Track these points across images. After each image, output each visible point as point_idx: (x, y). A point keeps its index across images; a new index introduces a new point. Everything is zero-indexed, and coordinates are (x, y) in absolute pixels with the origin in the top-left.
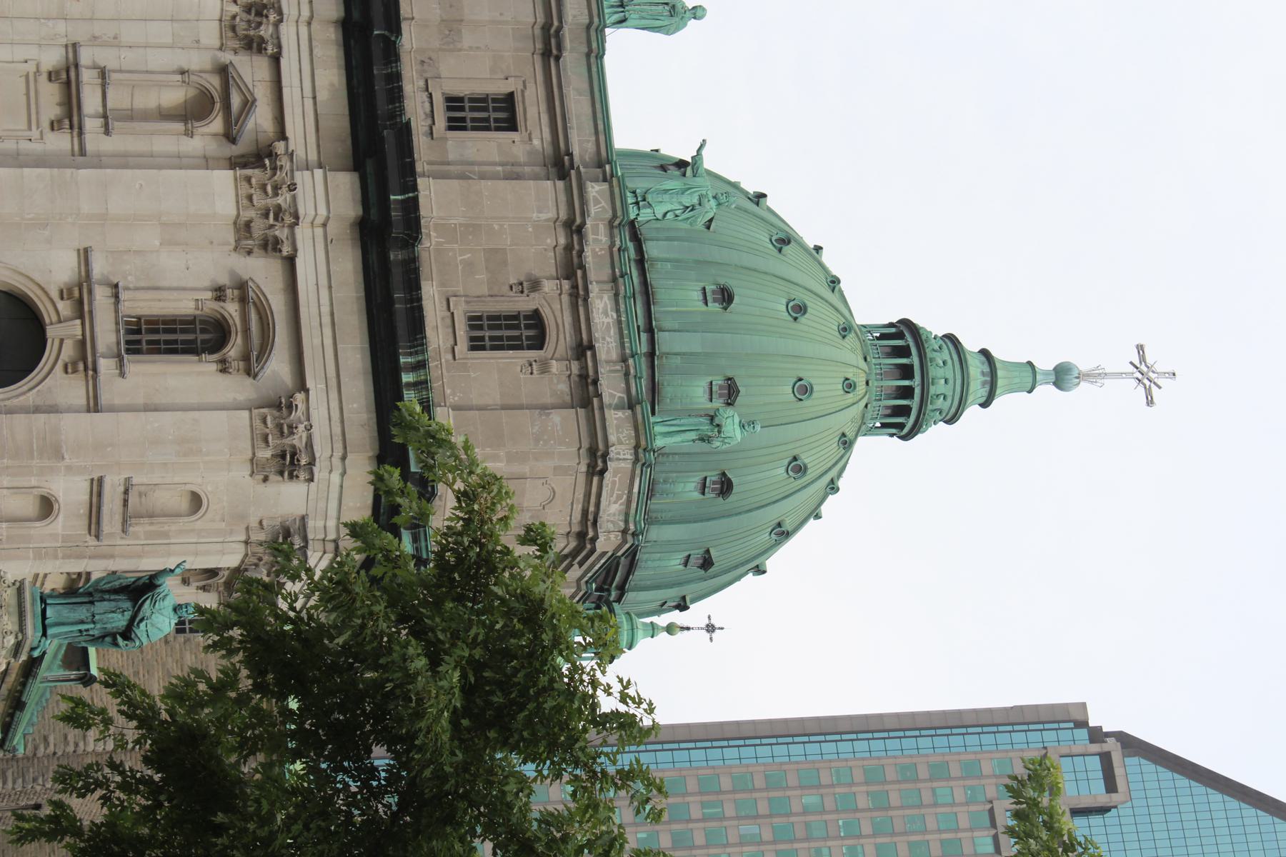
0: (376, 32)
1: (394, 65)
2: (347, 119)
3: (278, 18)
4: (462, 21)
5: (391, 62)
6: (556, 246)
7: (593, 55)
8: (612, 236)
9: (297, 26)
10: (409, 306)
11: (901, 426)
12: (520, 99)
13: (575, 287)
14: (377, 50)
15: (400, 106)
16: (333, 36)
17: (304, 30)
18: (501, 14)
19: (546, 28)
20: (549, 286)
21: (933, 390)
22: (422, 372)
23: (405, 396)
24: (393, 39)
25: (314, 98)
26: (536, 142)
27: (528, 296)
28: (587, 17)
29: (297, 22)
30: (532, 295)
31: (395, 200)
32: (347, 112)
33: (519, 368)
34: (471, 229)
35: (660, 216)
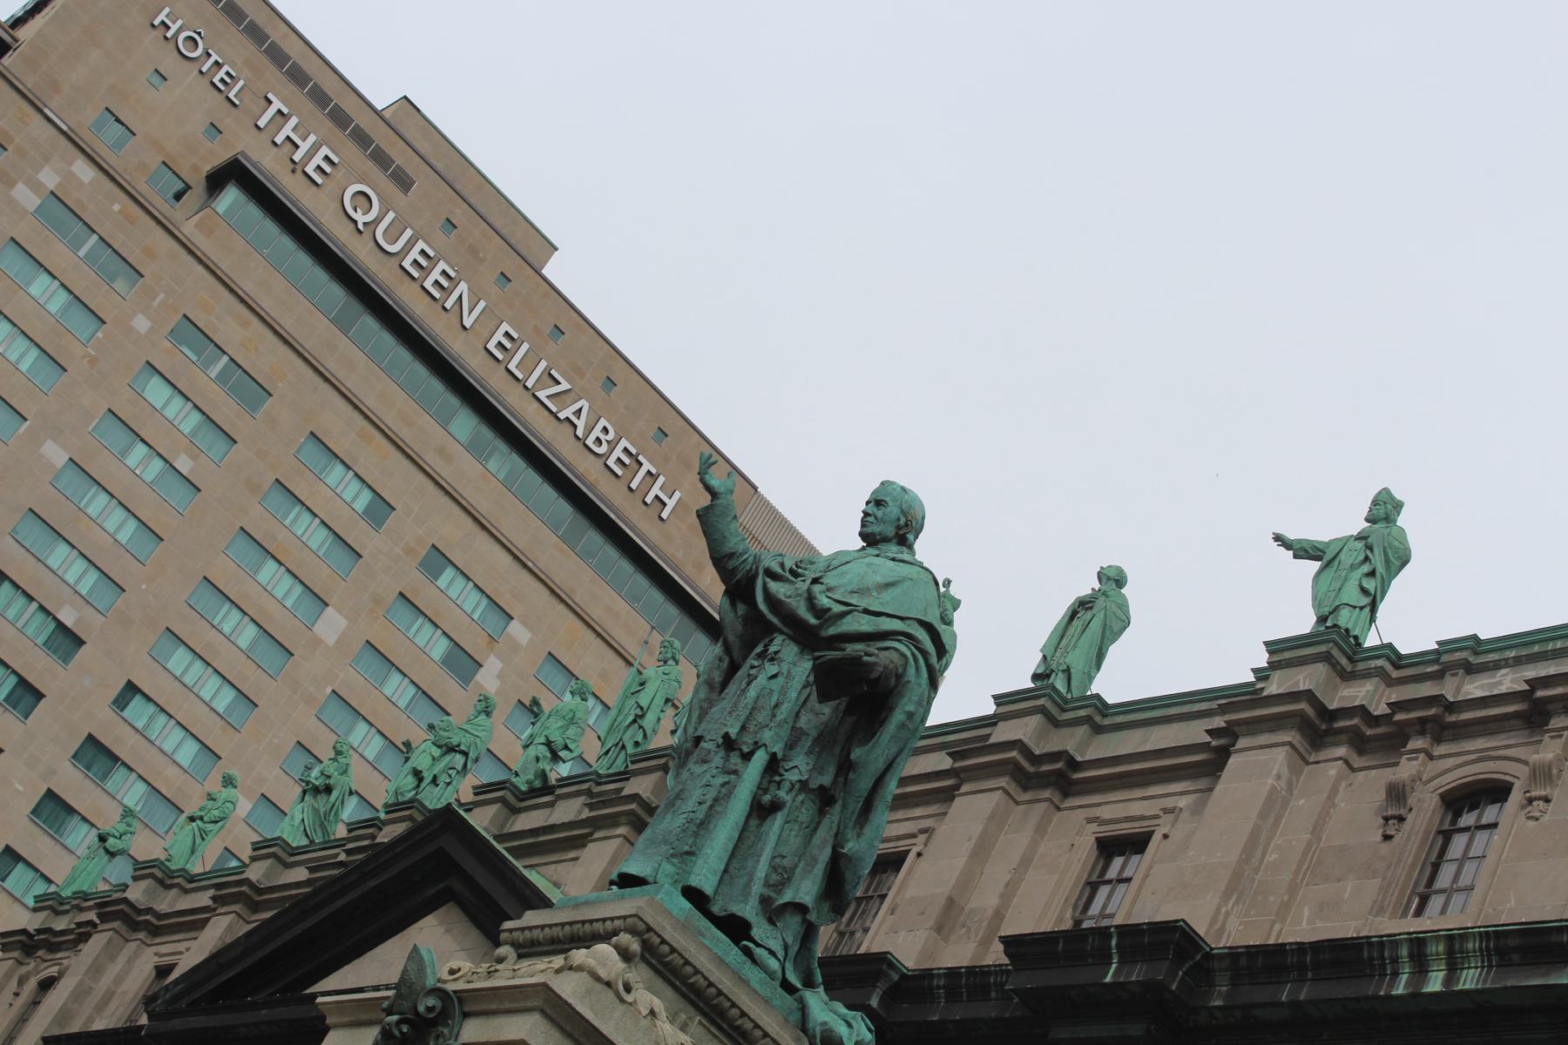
1: (935, 982)
4: (951, 902)
6: (1347, 762)
7: (1098, 719)
8: (1367, 675)
10: (1310, 975)
12: (1110, 827)
13: (1422, 726)
15: (996, 973)
19: (1026, 781)
20: (1406, 769)
22: (1431, 949)
23: (1467, 986)
24: (896, 977)
26: (1183, 802)
27: (1411, 810)
28: (1034, 717)
30: (1411, 801)
31: (1114, 975)
33: (1531, 823)
34: (1259, 898)
35: (1365, 601)
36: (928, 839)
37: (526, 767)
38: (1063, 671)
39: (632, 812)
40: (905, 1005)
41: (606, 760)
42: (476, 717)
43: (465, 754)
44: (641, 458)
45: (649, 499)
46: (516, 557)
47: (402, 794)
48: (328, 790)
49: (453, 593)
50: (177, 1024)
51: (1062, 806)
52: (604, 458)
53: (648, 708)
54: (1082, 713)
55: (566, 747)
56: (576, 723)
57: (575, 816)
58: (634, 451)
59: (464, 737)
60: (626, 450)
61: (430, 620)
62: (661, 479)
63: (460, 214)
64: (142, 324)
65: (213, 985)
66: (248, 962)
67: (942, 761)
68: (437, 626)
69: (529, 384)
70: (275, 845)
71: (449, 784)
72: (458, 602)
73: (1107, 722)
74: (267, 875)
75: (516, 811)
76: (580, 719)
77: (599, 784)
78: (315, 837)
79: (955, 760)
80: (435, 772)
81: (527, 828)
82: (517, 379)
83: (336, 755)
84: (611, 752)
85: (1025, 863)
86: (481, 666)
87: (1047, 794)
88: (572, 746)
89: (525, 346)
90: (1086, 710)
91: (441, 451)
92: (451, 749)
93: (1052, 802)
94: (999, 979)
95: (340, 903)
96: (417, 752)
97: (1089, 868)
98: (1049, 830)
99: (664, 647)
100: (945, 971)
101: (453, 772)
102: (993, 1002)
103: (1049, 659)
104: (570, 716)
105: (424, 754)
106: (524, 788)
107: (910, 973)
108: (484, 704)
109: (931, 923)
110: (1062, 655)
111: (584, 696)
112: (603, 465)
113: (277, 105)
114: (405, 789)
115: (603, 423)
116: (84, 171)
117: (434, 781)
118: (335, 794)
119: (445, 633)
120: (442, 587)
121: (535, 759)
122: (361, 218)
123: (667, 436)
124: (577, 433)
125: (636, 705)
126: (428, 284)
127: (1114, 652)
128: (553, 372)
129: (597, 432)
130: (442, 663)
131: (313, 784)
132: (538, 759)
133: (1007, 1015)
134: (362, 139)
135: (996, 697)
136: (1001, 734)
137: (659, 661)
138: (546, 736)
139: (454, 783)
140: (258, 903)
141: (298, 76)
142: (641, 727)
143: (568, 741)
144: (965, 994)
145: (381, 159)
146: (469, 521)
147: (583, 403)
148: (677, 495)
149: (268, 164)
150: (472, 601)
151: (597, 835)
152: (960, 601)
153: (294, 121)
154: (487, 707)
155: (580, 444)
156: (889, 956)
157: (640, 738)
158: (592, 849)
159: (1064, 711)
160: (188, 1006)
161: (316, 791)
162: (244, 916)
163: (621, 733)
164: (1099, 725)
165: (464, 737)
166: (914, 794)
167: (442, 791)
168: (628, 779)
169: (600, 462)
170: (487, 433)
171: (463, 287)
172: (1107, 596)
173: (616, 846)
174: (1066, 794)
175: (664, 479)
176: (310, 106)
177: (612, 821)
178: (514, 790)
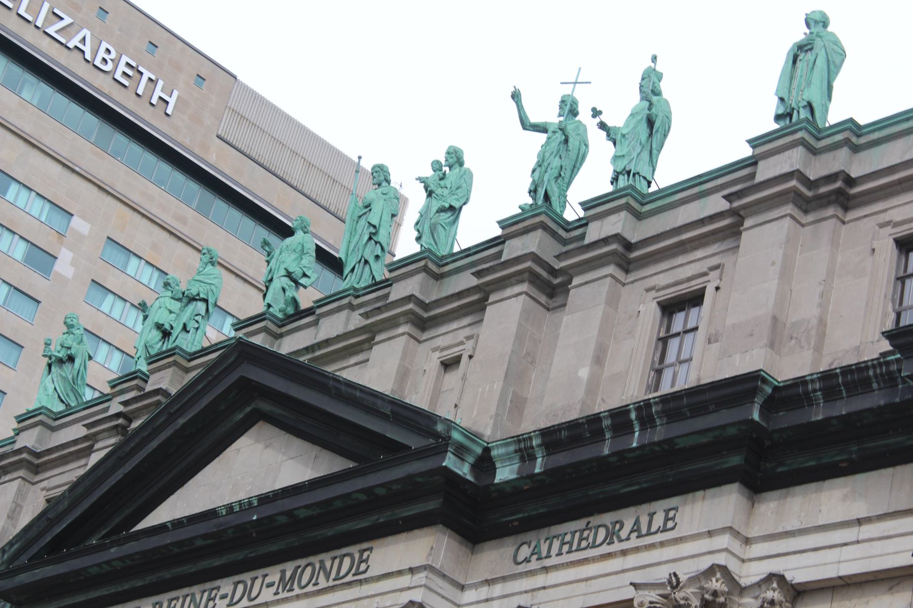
0: (756, 416)
1: (810, 387)
2: (899, 469)
3: (718, 575)
4: (775, 319)
5: (807, 393)
7: (854, 139)
9: (750, 560)
14: (787, 419)
15: (874, 366)
16: (773, 505)
17: (758, 549)
18: (773, 264)
19: (806, 205)
24: (769, 390)
25: (860, 522)
28: (795, 150)
29: (743, 561)
32: (890, 471)
36: (722, 273)
37: (275, 299)
38: (804, 107)
39: (411, 312)
40: (781, 413)
41: (353, 277)
42: (204, 269)
43: (206, 301)
44: (140, 69)
45: (154, 100)
46: (64, 165)
47: (152, 347)
48: (71, 359)
49: (21, 203)
50: (24, 578)
51: (846, 220)
52: (112, 74)
53: (379, 225)
54: (839, 137)
55: (305, 275)
56: (308, 253)
57: (344, 329)
58: (134, 64)
59: (200, 286)
60: (128, 64)
61: (8, 229)
62: (160, 83)
65: (48, 538)
66: (78, 512)
67: (716, 204)
68: (14, 233)
69: (39, 24)
70: (40, 414)
71: (197, 329)
72: (27, 210)
73: (863, 140)
74: (39, 440)
75: (281, 336)
76: (309, 249)
77: (357, 297)
78: (69, 401)
79: (730, 202)
80: (184, 320)
81: (301, 347)
82: (28, 21)
83: (68, 328)
84: (356, 270)
85: (830, 273)
86: (56, 258)
87: (830, 211)
88: (308, 273)
90: (841, 134)
92: (193, 299)
93: (838, 217)
94: (878, 371)
95: (154, 444)
96: (153, 310)
97: (895, 266)
98: (841, 242)
99: (376, 172)
100: (819, 375)
101: (199, 318)
102: (876, 392)
103: (786, 99)
104: (300, 248)
105: (162, 309)
106: (280, 316)
107: (781, 384)
108: (208, 256)
109: (765, 341)
110: (797, 93)
111: (306, 230)
112: (112, 81)
114: (153, 342)
115: (104, 45)
117: (185, 328)
118: (78, 361)
119: (21, 237)
120: (11, 200)
121: (281, 290)
123: (157, 47)
124: (86, 57)
125: (367, 224)
127: (838, 84)
128: (56, 11)
129: (102, 54)
130: (24, 262)
131: (55, 356)
132: (284, 290)
133: (897, 400)
135: (749, 142)
136: (765, 171)
137: (374, 184)
138: (285, 269)
139: (201, 327)
140: (38, 466)
142: (376, 243)
143: (305, 270)
144: (844, 391)
146: (20, 143)
147: (85, 32)
148: (176, 93)
150: (37, 207)
151: (378, 338)
152: (662, 74)
154: (211, 258)
155: (91, 66)
156: (762, 373)
157: (379, 252)
158: (378, 352)
159: (818, 139)
160: (29, 560)
161: (61, 361)
162: (29, 479)
163: (361, 251)
164: (856, 146)
165: (200, 286)
166: (690, 240)
167: (193, 336)
168: (391, 285)
169: (109, 78)
170: (16, 70)
172: (820, 37)
173: (403, 344)
174: (846, 209)
175: (162, 82)
177: (392, 323)
178: (273, 319)
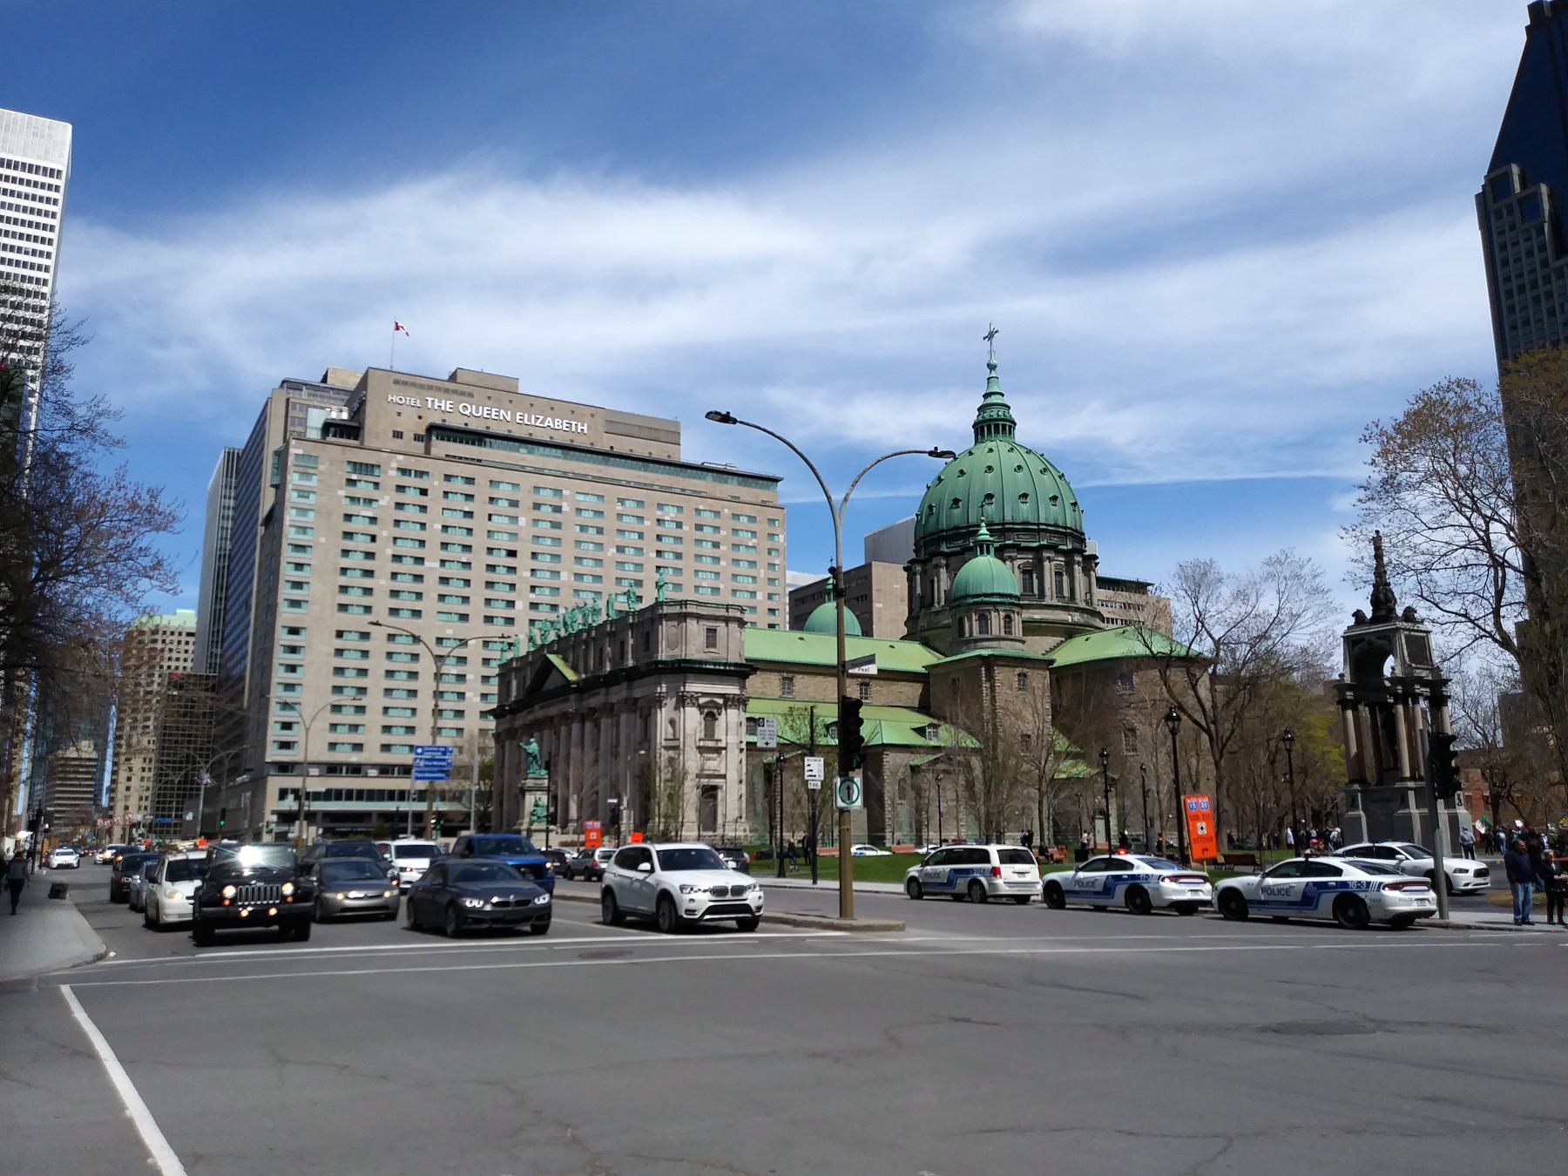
11: (1004, 426)
21: (996, 416)
63: (490, 393)
64: (436, 483)
89: (526, 415)
91: (524, 459)
113: (430, 399)
116: (400, 457)
122: (467, 413)
126: (493, 417)
134: (455, 392)
141: (430, 388)
145: (463, 394)
147: (549, 419)
149: (439, 422)
153: (436, 400)
171: (502, 412)
176: (438, 393)
